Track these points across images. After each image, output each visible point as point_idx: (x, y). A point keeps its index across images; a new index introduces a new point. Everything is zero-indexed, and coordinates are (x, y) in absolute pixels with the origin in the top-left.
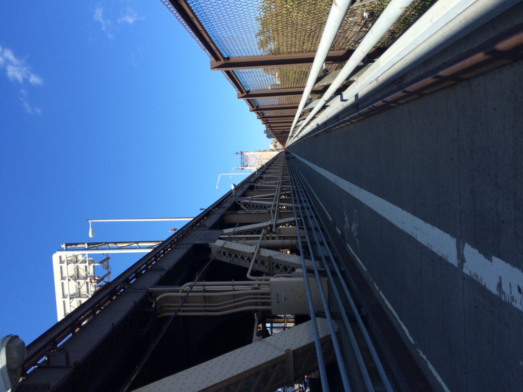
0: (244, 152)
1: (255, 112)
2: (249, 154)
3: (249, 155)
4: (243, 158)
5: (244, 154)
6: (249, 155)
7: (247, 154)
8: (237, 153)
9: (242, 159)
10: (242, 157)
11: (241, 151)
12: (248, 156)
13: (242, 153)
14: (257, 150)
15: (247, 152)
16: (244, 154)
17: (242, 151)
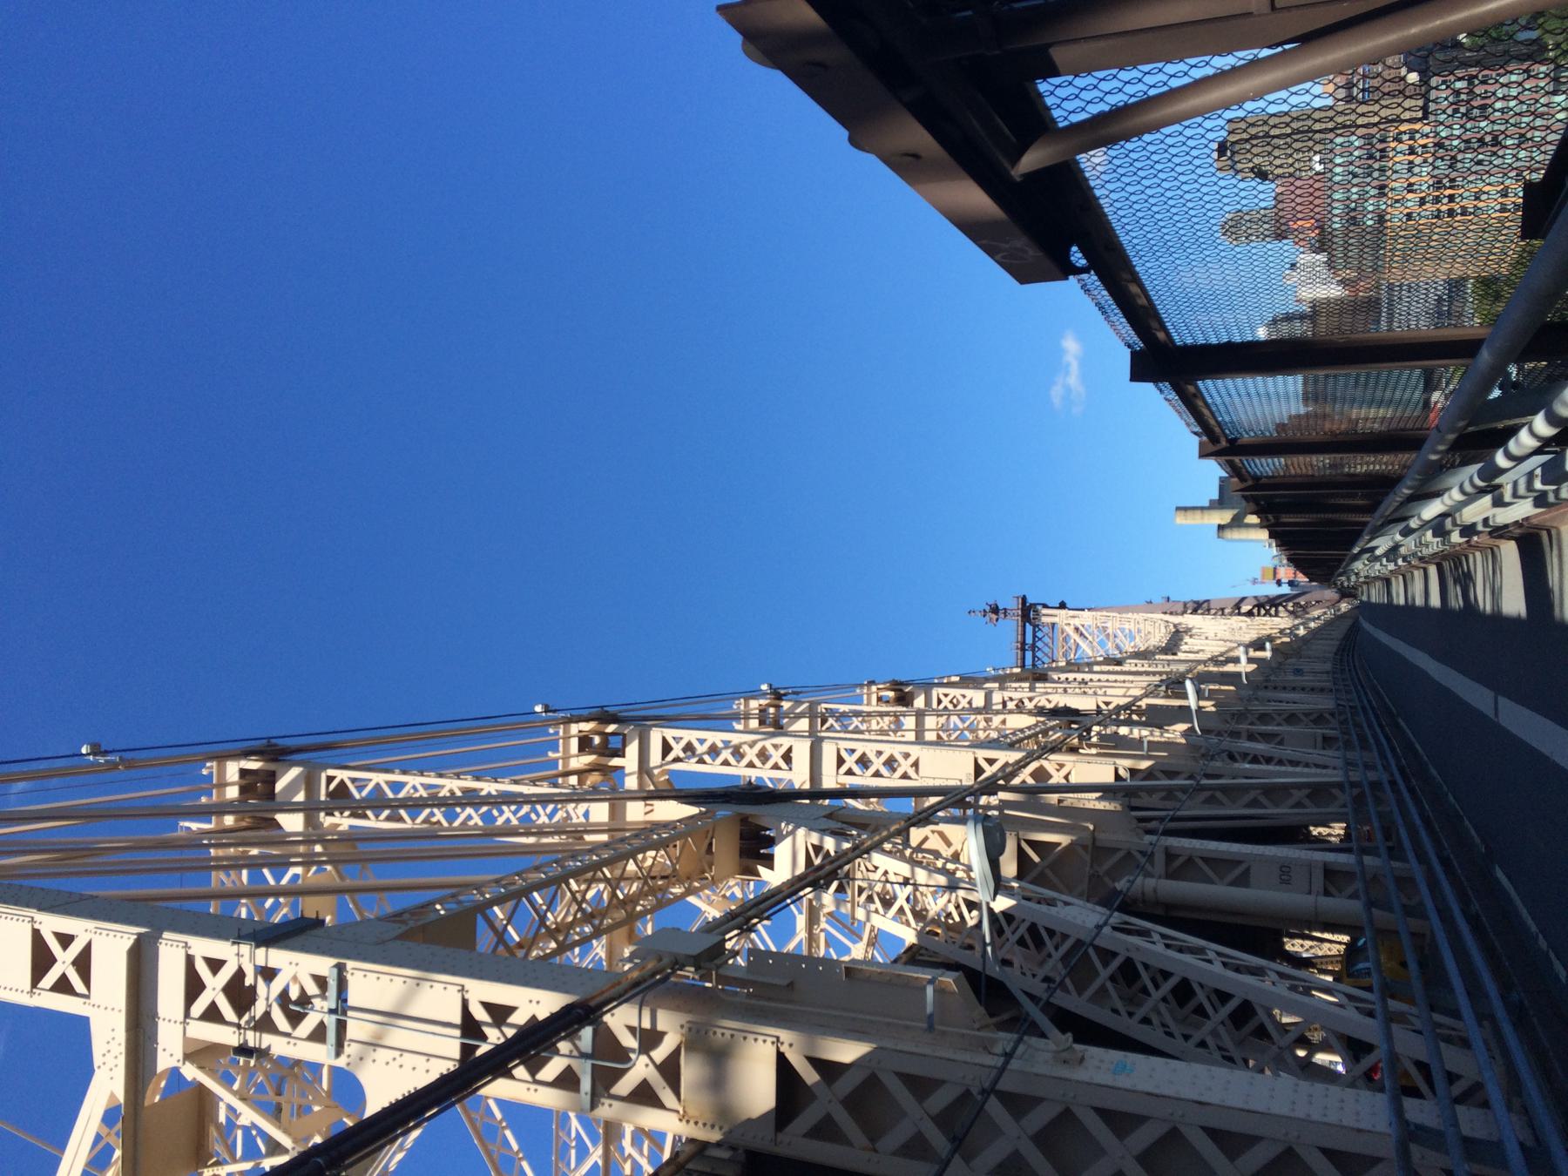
0: (1045, 606)
1: (1219, 459)
2: (1077, 622)
3: (1083, 626)
4: (1033, 646)
5: (1048, 617)
6: (1083, 626)
7: (1061, 617)
8: (995, 610)
9: (1029, 655)
10: (1029, 640)
11: (1024, 599)
12: (1066, 628)
13: (1028, 612)
14: (1158, 600)
15: (1063, 606)
16: (1044, 619)
17: (1030, 600)
